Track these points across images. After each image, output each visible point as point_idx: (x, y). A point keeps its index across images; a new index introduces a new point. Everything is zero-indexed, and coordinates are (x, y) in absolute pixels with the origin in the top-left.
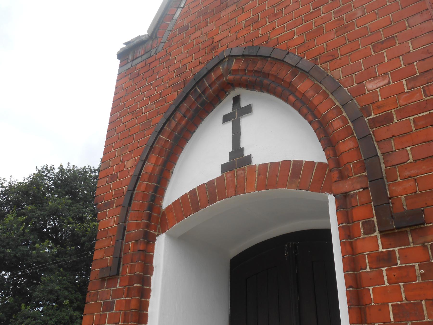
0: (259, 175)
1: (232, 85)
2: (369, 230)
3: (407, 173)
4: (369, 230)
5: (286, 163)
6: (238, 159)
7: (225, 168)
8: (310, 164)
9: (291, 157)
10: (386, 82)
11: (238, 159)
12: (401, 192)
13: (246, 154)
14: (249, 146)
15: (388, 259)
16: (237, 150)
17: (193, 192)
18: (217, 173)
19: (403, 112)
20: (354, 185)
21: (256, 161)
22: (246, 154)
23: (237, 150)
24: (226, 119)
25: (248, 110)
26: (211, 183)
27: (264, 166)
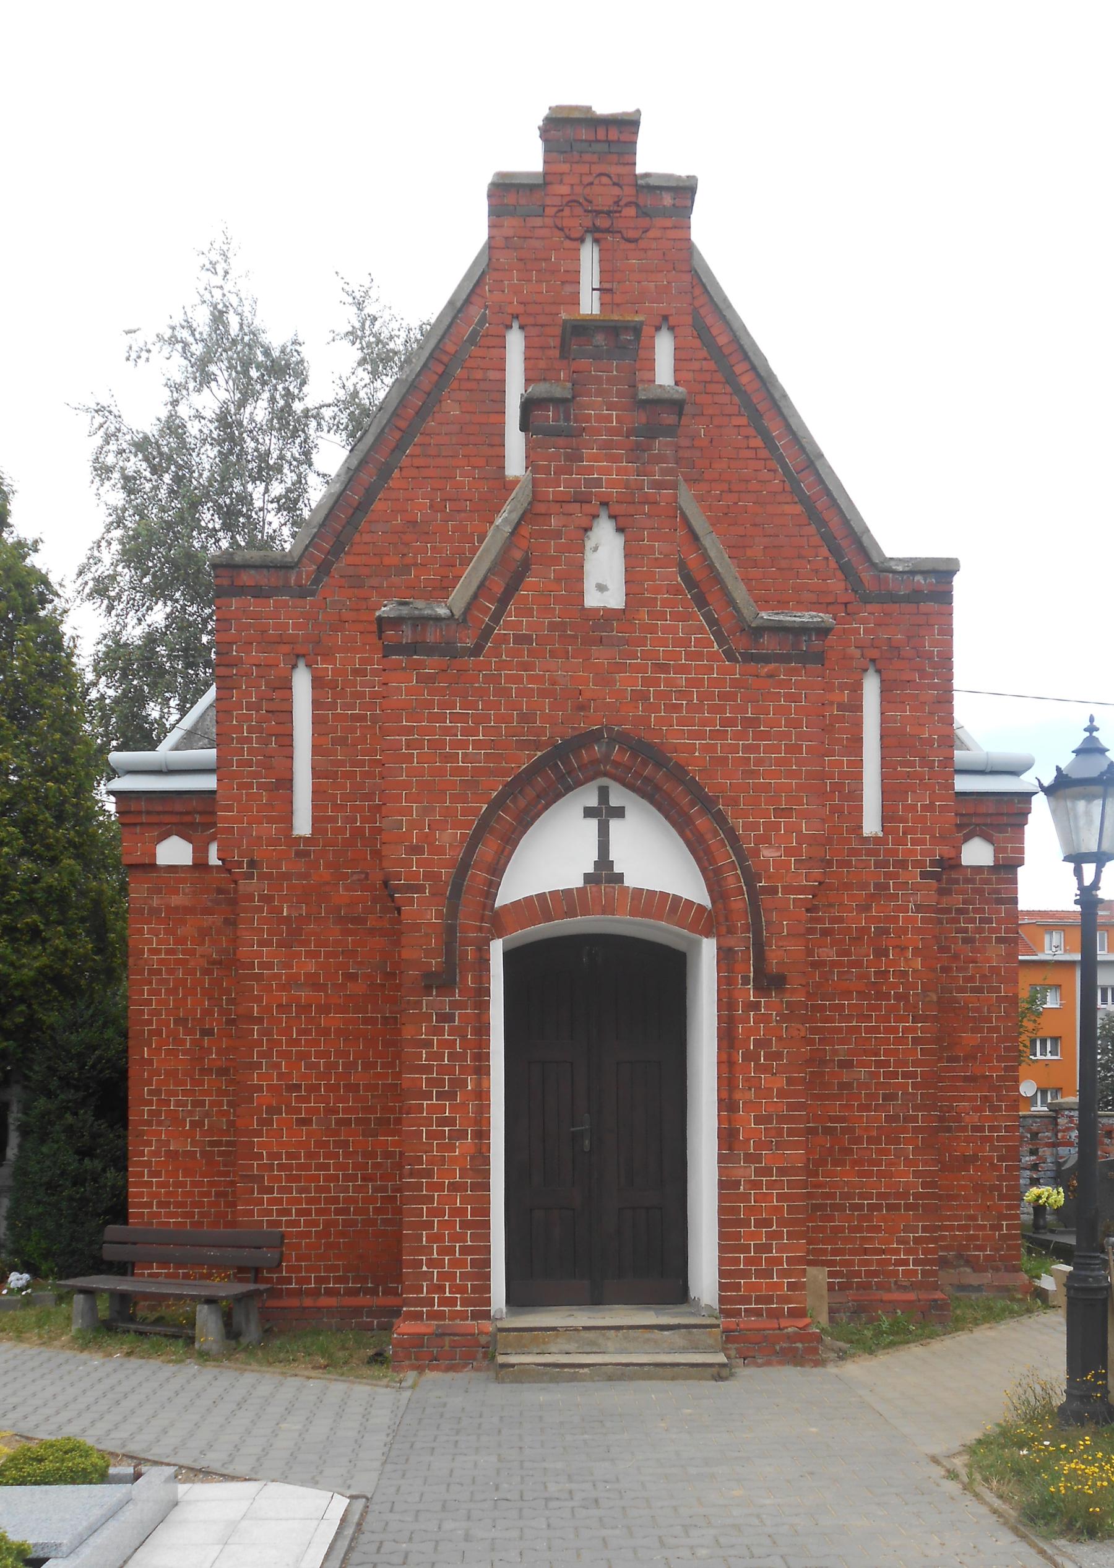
0: (632, 899)
1: (606, 774)
2: (746, 981)
3: (781, 944)
4: (746, 981)
5: (664, 895)
6: (604, 873)
7: (587, 877)
8: (689, 903)
9: (671, 890)
10: (779, 854)
11: (604, 873)
12: (775, 958)
13: (616, 870)
14: (622, 859)
15: (756, 1006)
16: (604, 861)
17: (541, 897)
18: (579, 883)
19: (788, 890)
20: (741, 942)
21: (630, 882)
22: (616, 870)
23: (604, 861)
24: (589, 813)
25: (620, 813)
26: (568, 892)
27: (638, 892)
